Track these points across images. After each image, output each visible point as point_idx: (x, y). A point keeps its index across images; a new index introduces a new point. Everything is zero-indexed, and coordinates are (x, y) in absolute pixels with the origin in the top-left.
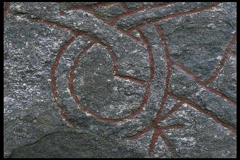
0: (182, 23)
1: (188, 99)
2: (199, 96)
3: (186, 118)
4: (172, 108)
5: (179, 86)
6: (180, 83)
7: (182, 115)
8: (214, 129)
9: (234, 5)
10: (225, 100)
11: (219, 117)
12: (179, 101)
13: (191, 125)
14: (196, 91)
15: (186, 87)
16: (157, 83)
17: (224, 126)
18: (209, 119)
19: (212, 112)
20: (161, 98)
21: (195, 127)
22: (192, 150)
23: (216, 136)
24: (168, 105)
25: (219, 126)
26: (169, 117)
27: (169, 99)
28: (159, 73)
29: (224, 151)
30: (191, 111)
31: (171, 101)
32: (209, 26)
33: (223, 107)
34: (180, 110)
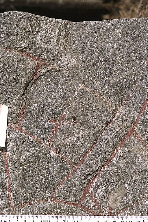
0: (17, 185)
1: (86, 187)
2: (85, 176)
3: (103, 190)
4: (93, 202)
5: (73, 194)
6: (70, 192)
7: (100, 194)
8: (117, 166)
9: (4, 147)
10: (90, 153)
11: (105, 160)
12: (87, 195)
13: (110, 186)
14: (80, 178)
15: (75, 188)
16: (69, 213)
17: (114, 156)
18: (106, 170)
19: (100, 166)
20: (82, 211)
21: (112, 183)
22: (133, 188)
23: (122, 166)
24: (90, 205)
25: (113, 161)
26: (100, 205)
27: (85, 203)
28: (59, 210)
29: (136, 160)
30: (98, 185)
31: (86, 202)
32: (22, 161)
33: (96, 156)
34: (95, 195)
